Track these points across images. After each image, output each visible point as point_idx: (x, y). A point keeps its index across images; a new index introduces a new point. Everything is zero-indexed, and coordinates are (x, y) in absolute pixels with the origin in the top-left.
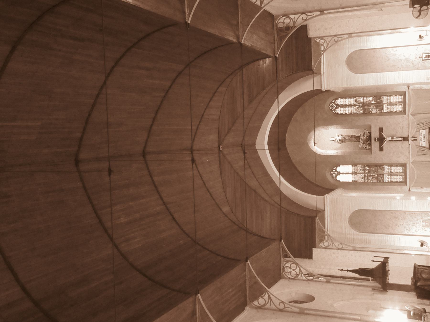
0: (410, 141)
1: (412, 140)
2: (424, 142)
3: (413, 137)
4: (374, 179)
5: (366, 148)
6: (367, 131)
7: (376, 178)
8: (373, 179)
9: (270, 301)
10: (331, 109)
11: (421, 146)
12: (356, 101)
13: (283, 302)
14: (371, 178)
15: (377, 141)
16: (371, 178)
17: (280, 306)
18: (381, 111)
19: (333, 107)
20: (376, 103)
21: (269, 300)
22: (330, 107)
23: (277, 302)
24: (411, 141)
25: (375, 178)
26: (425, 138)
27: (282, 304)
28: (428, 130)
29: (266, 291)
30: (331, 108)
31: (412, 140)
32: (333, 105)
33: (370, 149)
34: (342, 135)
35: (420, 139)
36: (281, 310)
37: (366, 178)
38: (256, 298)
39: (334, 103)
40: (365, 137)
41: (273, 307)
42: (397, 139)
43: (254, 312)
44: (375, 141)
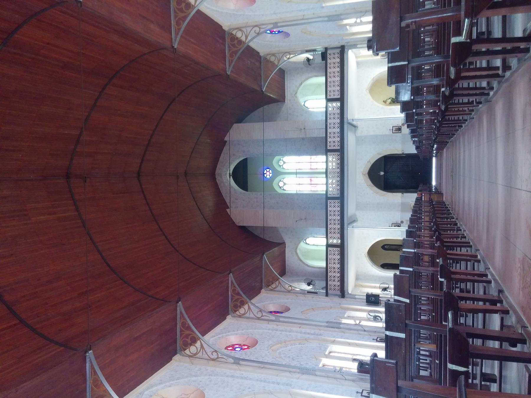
9: (202, 350)
13: (216, 351)
17: (212, 355)
21: (202, 350)
23: (209, 350)
27: (215, 354)
29: (199, 339)
36: (213, 360)
38: (186, 345)
41: (205, 356)
43: (187, 359)
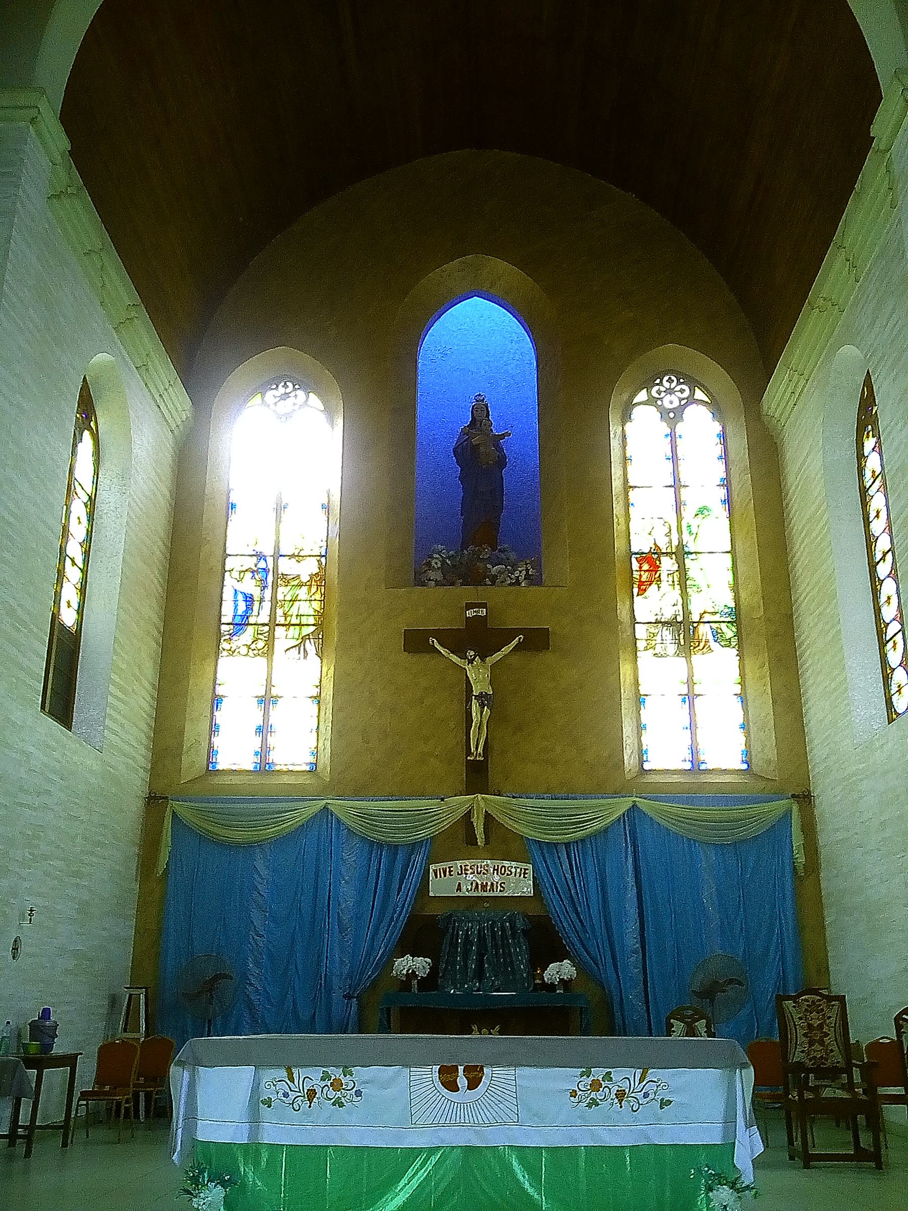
0: (460, 802)
1: (468, 815)
2: (459, 889)
3: (488, 816)
4: (242, 607)
5: (429, 564)
6: (527, 570)
7: (246, 616)
8: (240, 597)
10: (658, 381)
11: (432, 867)
12: (702, 511)
14: (250, 586)
15: (470, 613)
16: (250, 586)
18: (641, 645)
19: (670, 391)
20: (695, 617)
22: (666, 378)
24: (463, 810)
25: (246, 611)
26: (481, 893)
28: (534, 910)
30: (661, 384)
31: (468, 815)
32: (679, 394)
33: (420, 581)
34: (501, 462)
35: (479, 863)
37: (251, 563)
39: (691, 400)
40: (489, 566)
42: (476, 727)
44: (469, 606)
